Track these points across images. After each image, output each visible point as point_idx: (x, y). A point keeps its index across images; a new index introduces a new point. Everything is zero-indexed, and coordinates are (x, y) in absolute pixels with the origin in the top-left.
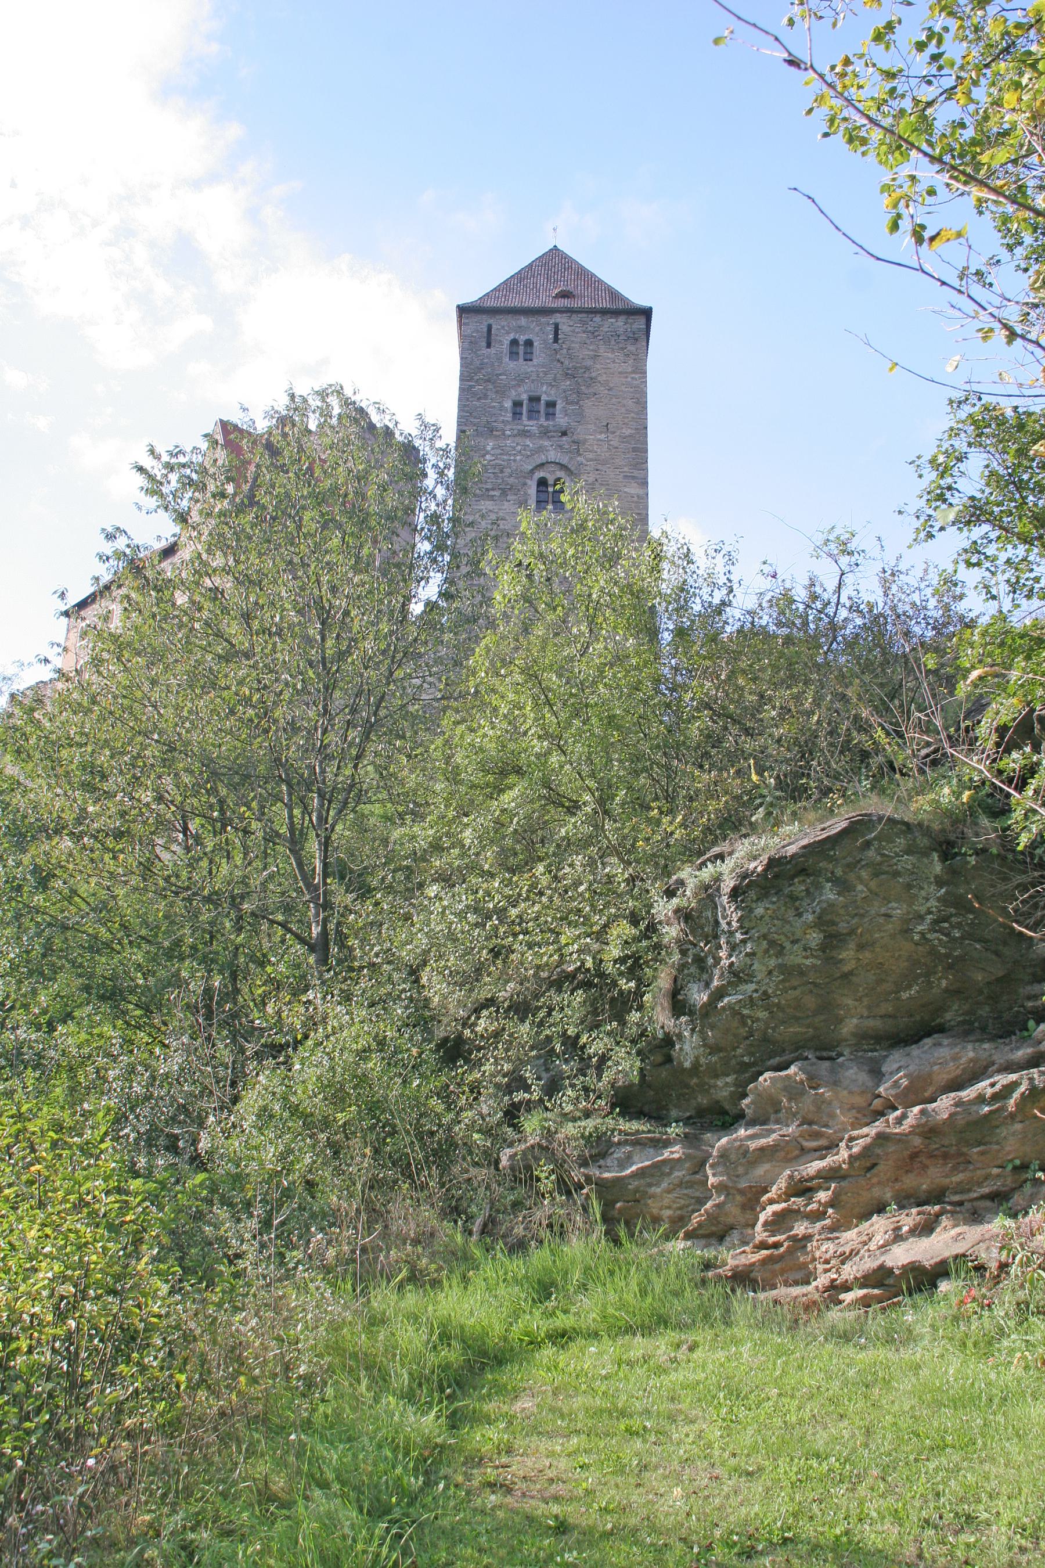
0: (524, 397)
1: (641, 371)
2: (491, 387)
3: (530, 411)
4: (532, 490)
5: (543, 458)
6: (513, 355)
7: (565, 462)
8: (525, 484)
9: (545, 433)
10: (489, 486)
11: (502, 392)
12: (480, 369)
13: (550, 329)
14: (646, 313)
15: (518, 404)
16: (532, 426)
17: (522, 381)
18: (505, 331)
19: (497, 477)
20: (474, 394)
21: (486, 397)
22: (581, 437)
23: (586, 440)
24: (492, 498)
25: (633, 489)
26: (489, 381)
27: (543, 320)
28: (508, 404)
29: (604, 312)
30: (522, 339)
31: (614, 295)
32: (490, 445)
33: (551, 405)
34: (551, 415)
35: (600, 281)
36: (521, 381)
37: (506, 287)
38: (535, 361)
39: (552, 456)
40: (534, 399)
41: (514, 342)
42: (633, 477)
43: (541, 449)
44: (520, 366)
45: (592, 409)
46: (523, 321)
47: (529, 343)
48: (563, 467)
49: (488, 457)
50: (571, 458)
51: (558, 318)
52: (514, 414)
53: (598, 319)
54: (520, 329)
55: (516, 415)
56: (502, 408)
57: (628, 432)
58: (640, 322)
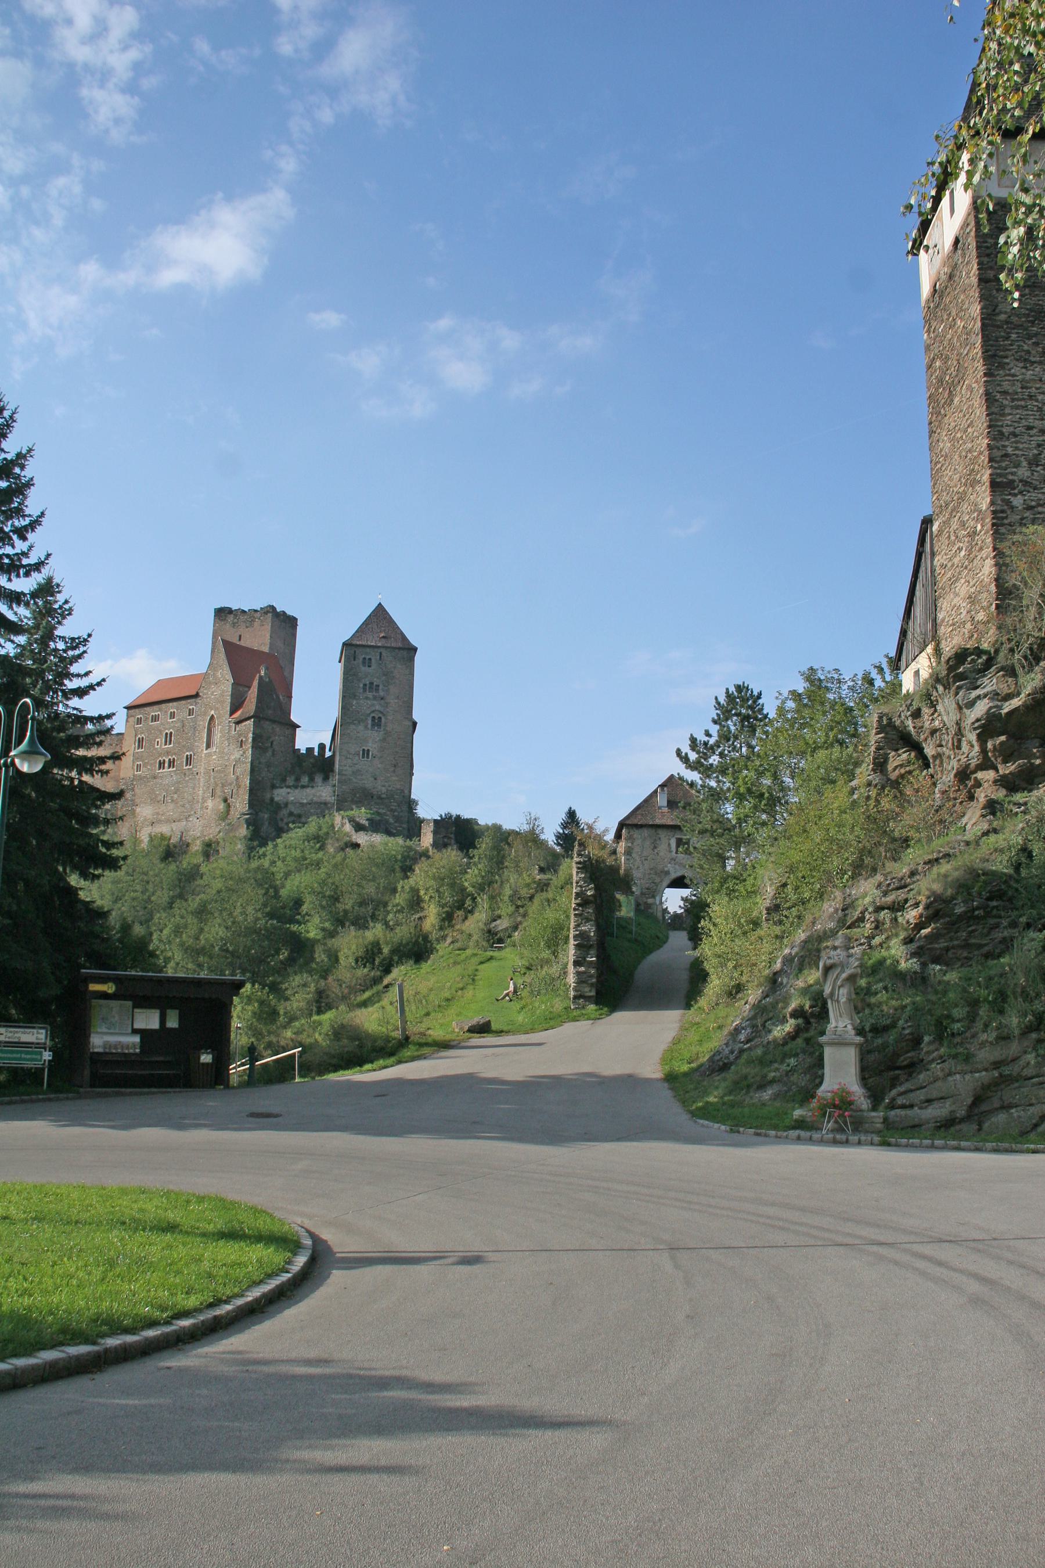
1: (412, 674)
3: (370, 688)
4: (370, 722)
6: (364, 663)
7: (382, 709)
9: (375, 698)
11: (359, 680)
13: (378, 654)
14: (415, 649)
15: (365, 685)
16: (370, 695)
24: (354, 724)
27: (376, 650)
28: (361, 685)
29: (399, 649)
30: (368, 657)
31: (404, 638)
32: (354, 702)
33: (378, 686)
34: (377, 690)
35: (398, 627)
37: (361, 631)
38: (373, 667)
39: (377, 707)
40: (371, 683)
41: (364, 659)
43: (373, 705)
46: (368, 650)
47: (370, 659)
48: (382, 713)
51: (382, 650)
53: (397, 651)
54: (366, 653)
55: (365, 690)
58: (413, 652)
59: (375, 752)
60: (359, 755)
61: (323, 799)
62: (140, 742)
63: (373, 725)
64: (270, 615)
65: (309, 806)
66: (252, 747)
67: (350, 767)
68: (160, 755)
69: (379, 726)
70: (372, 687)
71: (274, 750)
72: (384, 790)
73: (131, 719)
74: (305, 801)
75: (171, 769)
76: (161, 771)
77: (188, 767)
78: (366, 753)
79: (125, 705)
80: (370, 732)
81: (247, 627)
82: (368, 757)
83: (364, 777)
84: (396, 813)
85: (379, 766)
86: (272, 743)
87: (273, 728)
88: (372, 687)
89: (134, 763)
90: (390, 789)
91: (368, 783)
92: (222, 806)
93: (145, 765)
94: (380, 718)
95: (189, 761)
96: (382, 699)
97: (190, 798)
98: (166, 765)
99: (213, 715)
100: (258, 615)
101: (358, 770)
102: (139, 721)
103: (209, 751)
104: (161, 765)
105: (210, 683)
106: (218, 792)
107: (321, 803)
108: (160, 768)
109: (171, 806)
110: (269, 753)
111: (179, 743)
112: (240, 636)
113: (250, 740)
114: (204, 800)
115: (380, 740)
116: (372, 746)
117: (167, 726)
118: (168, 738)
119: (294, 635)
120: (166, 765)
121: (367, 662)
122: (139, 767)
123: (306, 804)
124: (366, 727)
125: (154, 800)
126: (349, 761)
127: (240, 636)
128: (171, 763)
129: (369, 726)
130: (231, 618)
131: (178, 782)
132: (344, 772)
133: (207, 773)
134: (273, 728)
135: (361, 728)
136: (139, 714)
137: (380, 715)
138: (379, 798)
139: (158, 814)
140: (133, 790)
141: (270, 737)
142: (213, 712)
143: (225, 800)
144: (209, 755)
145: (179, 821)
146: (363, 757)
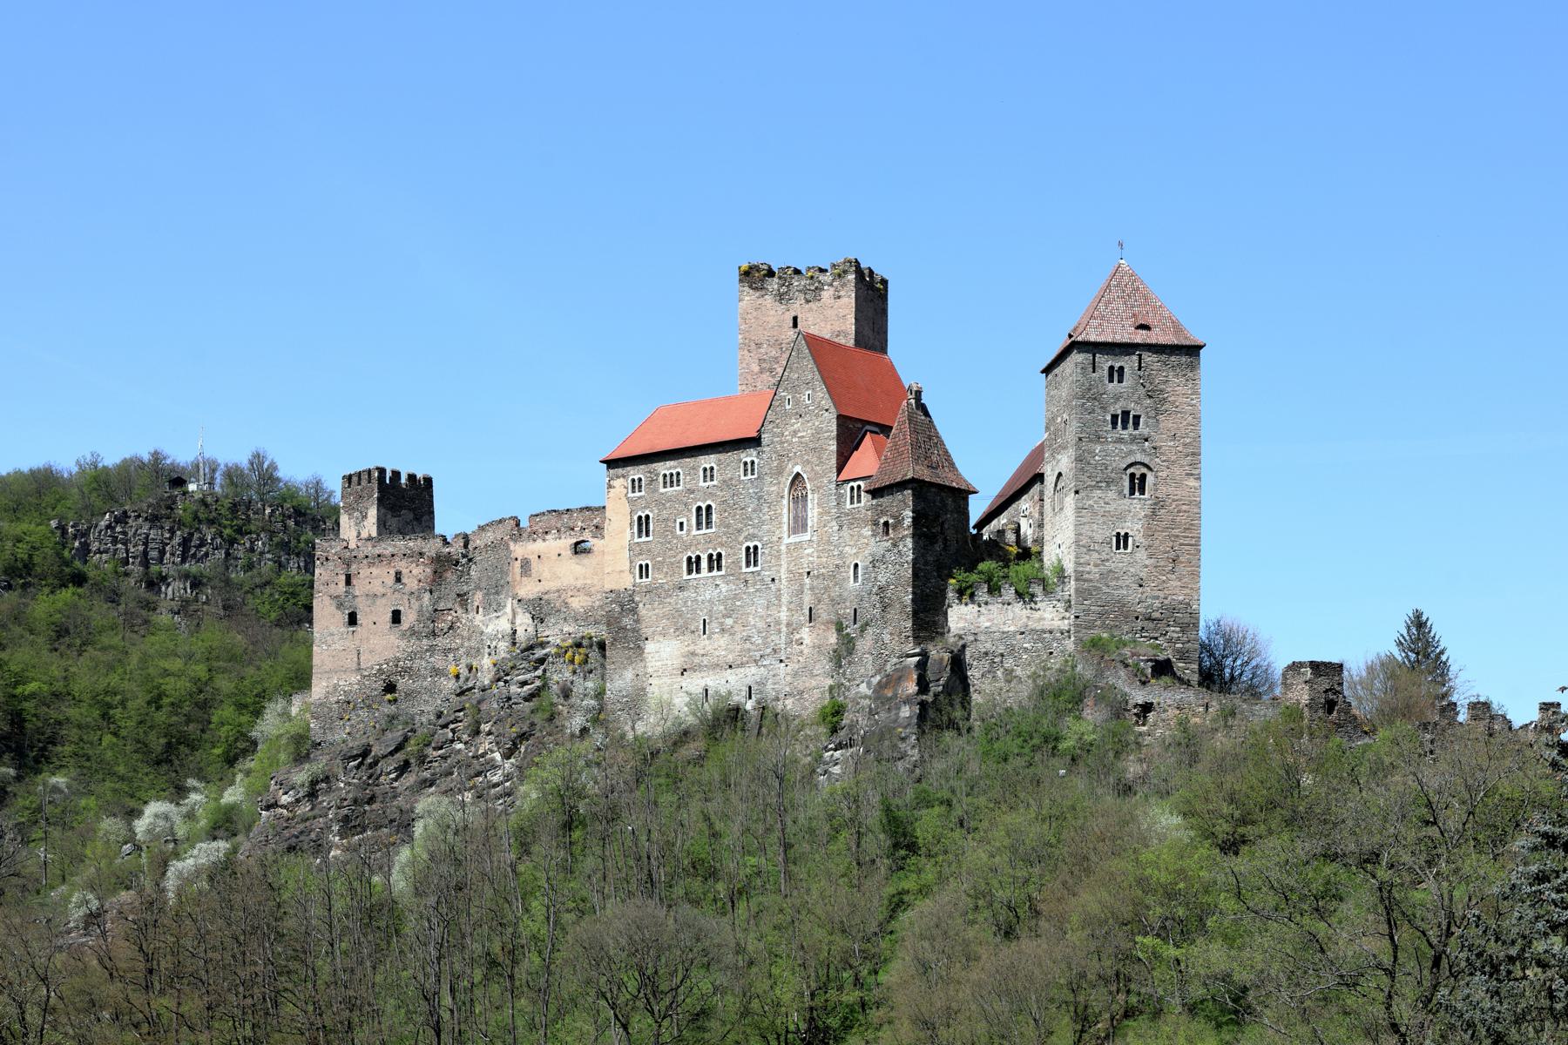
0: (1119, 412)
2: (1097, 404)
4: (1127, 484)
5: (1131, 460)
7: (1146, 461)
8: (1121, 478)
9: (1133, 439)
10: (1098, 479)
12: (1090, 389)
15: (1114, 417)
16: (1125, 434)
17: (1118, 399)
18: (1105, 362)
19: (1103, 473)
20: (1087, 409)
21: (1093, 411)
22: (1158, 444)
23: (1161, 447)
25: (1192, 483)
26: (1095, 399)
28: (1109, 418)
32: (1098, 448)
33: (1137, 418)
34: (1136, 425)
36: (1117, 398)
39: (1139, 457)
40: (1126, 414)
42: (1192, 475)
43: (1131, 452)
44: (1113, 387)
45: (1167, 423)
49: (1097, 458)
50: (1151, 460)
52: (1112, 423)
55: (1114, 424)
56: (1105, 421)
57: (1188, 440)
59: (1139, 538)
60: (1110, 543)
61: (1047, 625)
62: (643, 525)
63: (1132, 493)
64: (852, 277)
65: (1019, 637)
66: (914, 535)
67: (1096, 565)
68: (687, 548)
69: (1142, 492)
70: (1125, 419)
71: (945, 539)
72: (1157, 604)
73: (618, 483)
74: (1012, 629)
75: (715, 573)
76: (694, 575)
77: (752, 569)
78: (1122, 540)
79: (604, 456)
80: (1127, 501)
81: (808, 301)
82: (1126, 547)
83: (1120, 583)
84: (1180, 645)
85: (1147, 562)
86: (943, 524)
87: (942, 501)
88: (1125, 419)
89: (631, 562)
90: (1166, 602)
91: (1132, 595)
92: (833, 638)
93: (658, 569)
94: (1143, 476)
95: (752, 555)
96: (1146, 440)
97: (761, 625)
98: (704, 564)
99: (798, 474)
100: (827, 278)
101: (1111, 571)
102: (636, 485)
103: (794, 539)
104: (693, 564)
105: (786, 414)
106: (823, 613)
107: (1044, 632)
108: (690, 572)
109: (723, 641)
110: (938, 547)
111: (728, 526)
112: (795, 319)
113: (908, 521)
114: (793, 628)
115: (1146, 516)
116: (1134, 528)
117: (698, 495)
118: (704, 516)
119: (884, 312)
120: (704, 564)
121: (1116, 374)
122: (644, 570)
123: (1015, 632)
124: (1120, 492)
125: (682, 630)
126: (1095, 555)
127: (795, 319)
128: (715, 562)
129: (1127, 491)
130: (773, 284)
131: (736, 597)
132: (1087, 576)
133: (795, 577)
134: (942, 501)
135: (1112, 495)
136: (636, 472)
137: (1144, 470)
138: (1150, 619)
139: (693, 654)
140: (634, 611)
141: (938, 516)
142: (798, 469)
143: (840, 628)
144: (798, 545)
145: (742, 665)
146: (1118, 547)
